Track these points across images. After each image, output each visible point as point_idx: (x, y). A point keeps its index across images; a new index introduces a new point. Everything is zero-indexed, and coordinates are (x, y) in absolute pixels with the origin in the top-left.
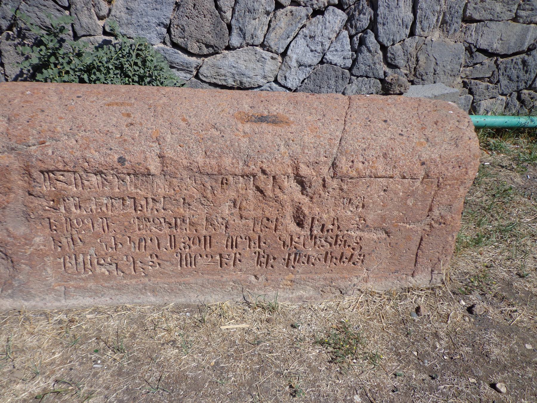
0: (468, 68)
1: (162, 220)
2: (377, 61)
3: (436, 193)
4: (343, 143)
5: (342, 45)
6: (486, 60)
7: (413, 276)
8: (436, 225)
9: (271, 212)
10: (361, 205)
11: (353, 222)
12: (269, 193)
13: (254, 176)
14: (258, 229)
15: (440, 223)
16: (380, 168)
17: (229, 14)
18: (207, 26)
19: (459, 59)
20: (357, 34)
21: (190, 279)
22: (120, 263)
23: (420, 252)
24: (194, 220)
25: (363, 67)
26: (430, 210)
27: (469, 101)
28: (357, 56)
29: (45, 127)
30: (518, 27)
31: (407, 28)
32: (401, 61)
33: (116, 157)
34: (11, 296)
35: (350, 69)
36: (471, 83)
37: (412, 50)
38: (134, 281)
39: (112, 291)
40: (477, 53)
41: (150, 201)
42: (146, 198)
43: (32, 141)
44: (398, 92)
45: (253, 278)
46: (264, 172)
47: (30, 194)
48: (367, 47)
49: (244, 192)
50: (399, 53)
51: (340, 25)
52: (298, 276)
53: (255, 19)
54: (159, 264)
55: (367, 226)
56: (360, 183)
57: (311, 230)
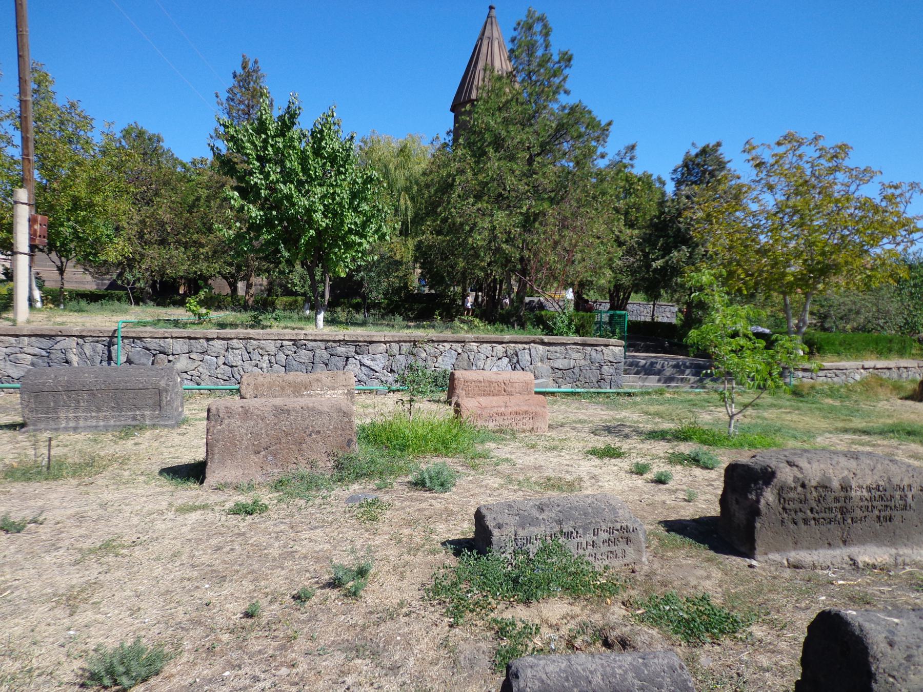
6: (560, 372)
18: (466, 364)
30: (567, 361)
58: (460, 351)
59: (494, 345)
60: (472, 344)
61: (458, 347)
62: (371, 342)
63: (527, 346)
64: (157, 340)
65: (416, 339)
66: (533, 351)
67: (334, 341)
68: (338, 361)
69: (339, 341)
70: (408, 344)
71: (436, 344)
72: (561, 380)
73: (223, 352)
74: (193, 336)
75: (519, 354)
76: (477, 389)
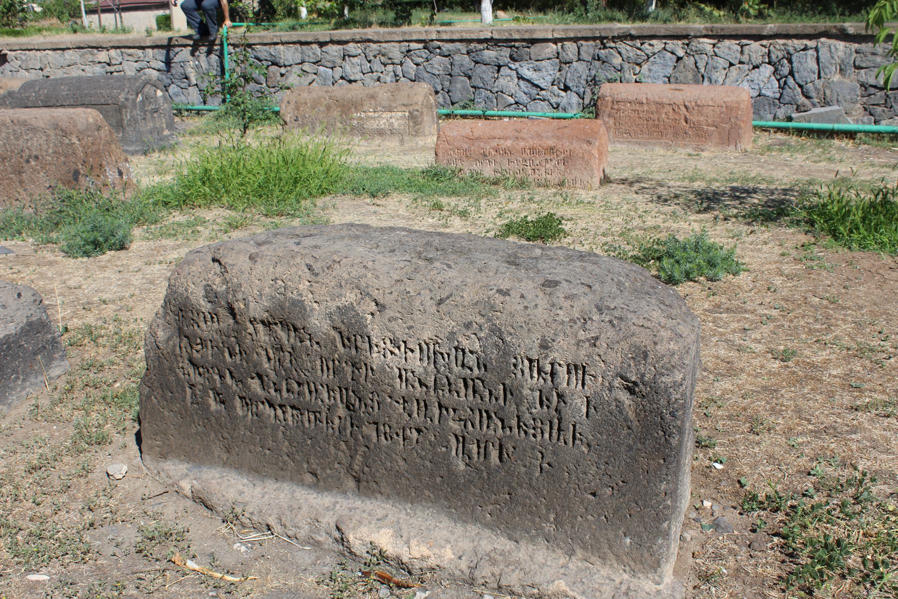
5: (772, 85)
9: (677, 117)
16: (711, 103)
17: (702, 70)
20: (781, 78)
31: (814, 73)
32: (813, 94)
35: (779, 99)
37: (820, 87)
58: (681, 53)
59: (745, 41)
60: (702, 40)
61: (678, 47)
62: (533, 42)
63: (811, 43)
64: (267, 48)
65: (603, 34)
66: (824, 54)
67: (480, 41)
68: (484, 72)
69: (486, 41)
70: (591, 43)
71: (638, 43)
72: (879, 109)
73: (339, 61)
74: (303, 40)
75: (794, 58)
76: (633, 115)
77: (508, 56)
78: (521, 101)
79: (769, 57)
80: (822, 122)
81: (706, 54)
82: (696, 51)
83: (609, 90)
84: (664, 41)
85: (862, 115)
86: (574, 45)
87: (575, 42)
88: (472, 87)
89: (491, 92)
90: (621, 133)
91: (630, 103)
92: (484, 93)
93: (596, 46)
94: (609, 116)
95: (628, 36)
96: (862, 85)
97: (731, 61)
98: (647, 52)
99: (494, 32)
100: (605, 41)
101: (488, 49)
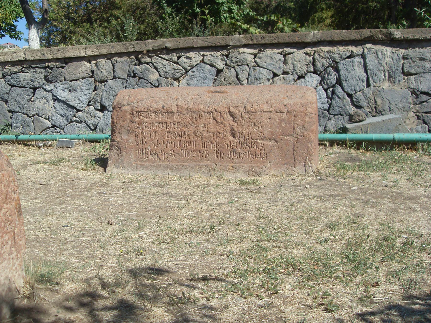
0: (417, 106)
1: (176, 133)
2: (346, 104)
3: (294, 120)
4: (249, 98)
7: (295, 167)
8: (300, 137)
9: (220, 129)
10: (260, 126)
11: (258, 135)
12: (219, 120)
13: (212, 113)
14: (215, 137)
15: (302, 136)
19: (407, 99)
20: (329, 88)
21: (187, 164)
22: (159, 153)
23: (295, 153)
24: (189, 133)
25: (337, 108)
26: (294, 129)
27: (425, 129)
28: (331, 101)
29: (140, 97)
31: (363, 82)
32: (364, 103)
33: (162, 105)
34: (117, 167)
35: (328, 111)
36: (422, 116)
37: (370, 95)
38: (163, 163)
39: (154, 168)
40: (421, 95)
41: (172, 124)
42: (171, 123)
43: (135, 101)
44: (358, 120)
45: (215, 165)
46: (216, 111)
47: (131, 122)
48: (336, 95)
49: (208, 120)
50: (360, 98)
51: (316, 83)
52: (235, 164)
53: (260, 83)
54: (174, 155)
55: (265, 137)
56: (257, 115)
57: (239, 139)
58: (220, 65)
60: (242, 50)
63: (357, 50)
66: (371, 60)
67: (14, 63)
70: (126, 59)
71: (174, 56)
75: (341, 66)
76: (160, 129)
77: (42, 77)
78: (58, 124)
79: (314, 65)
80: (380, 132)
81: (248, 65)
82: (237, 62)
83: (127, 97)
84: (202, 53)
85: (415, 124)
86: (109, 62)
87: (109, 59)
88: (9, 111)
89: (28, 116)
90: (146, 155)
91: (155, 112)
92: (21, 117)
93: (131, 62)
94: (129, 132)
95: (163, 49)
96: (413, 92)
97: (275, 71)
98: (185, 65)
99: (27, 53)
100: (140, 56)
101: (23, 71)
